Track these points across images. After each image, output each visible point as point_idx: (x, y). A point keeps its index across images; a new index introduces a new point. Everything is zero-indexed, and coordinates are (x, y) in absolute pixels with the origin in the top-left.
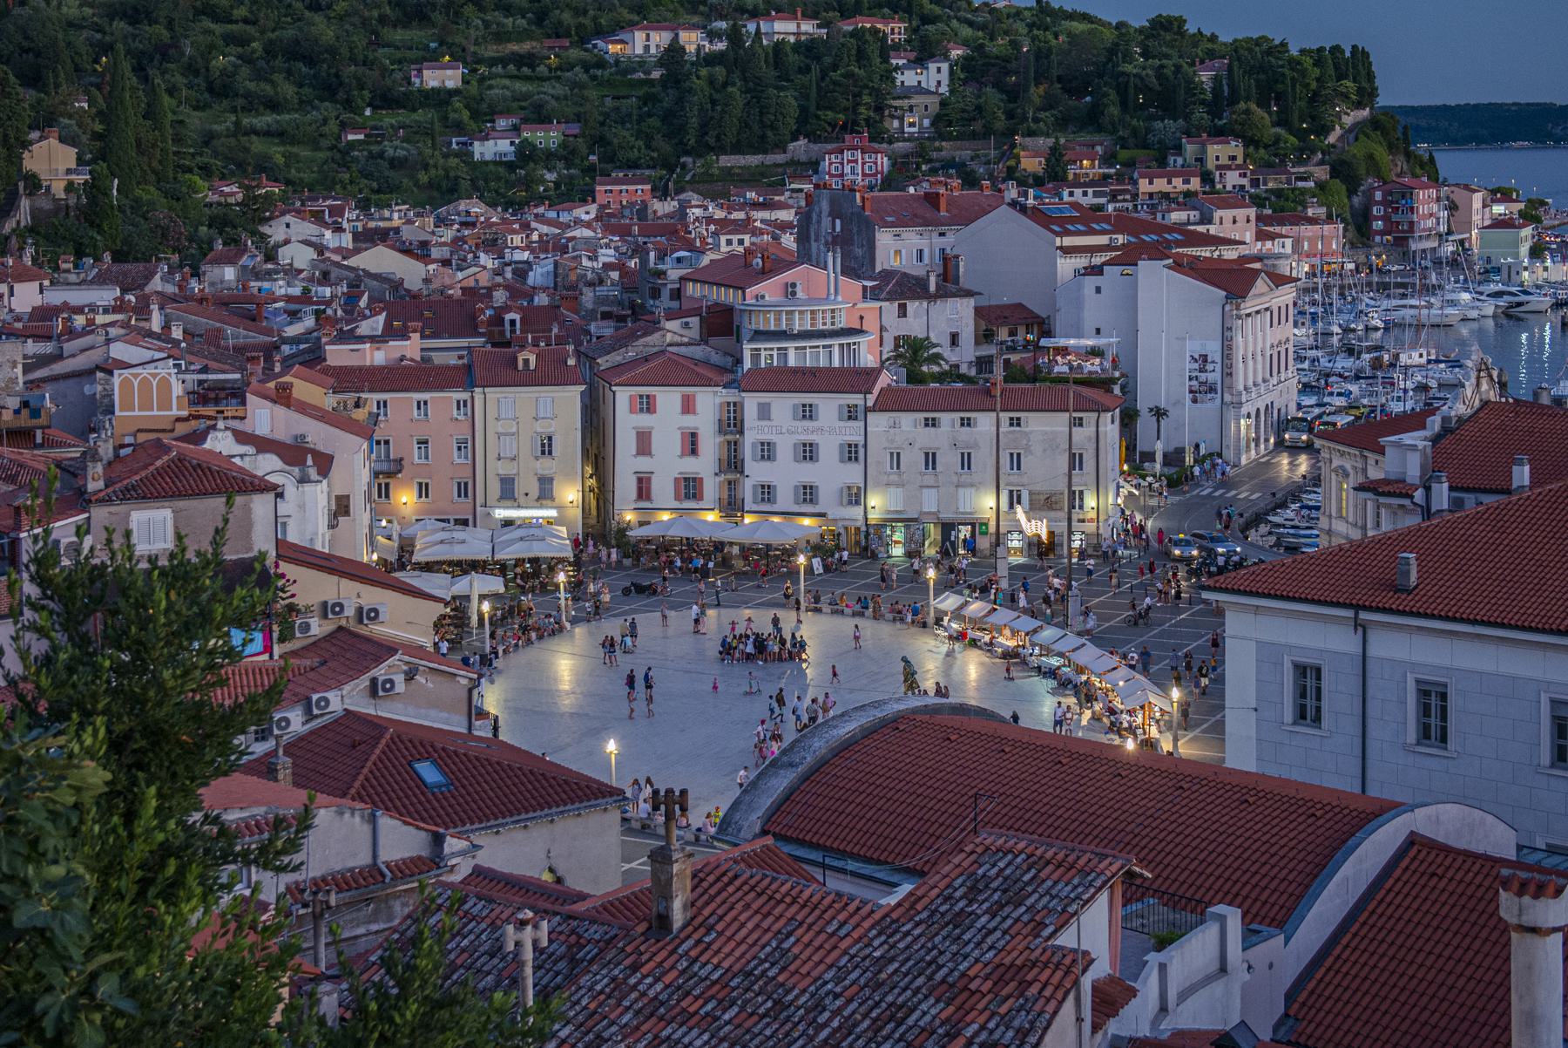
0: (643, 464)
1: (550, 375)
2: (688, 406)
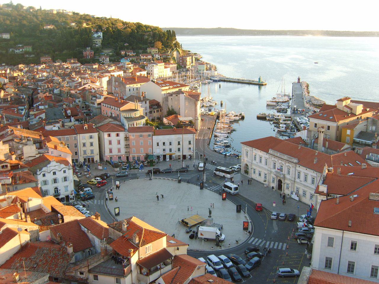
0: (110, 146)
1: (90, 130)
2: (118, 135)
